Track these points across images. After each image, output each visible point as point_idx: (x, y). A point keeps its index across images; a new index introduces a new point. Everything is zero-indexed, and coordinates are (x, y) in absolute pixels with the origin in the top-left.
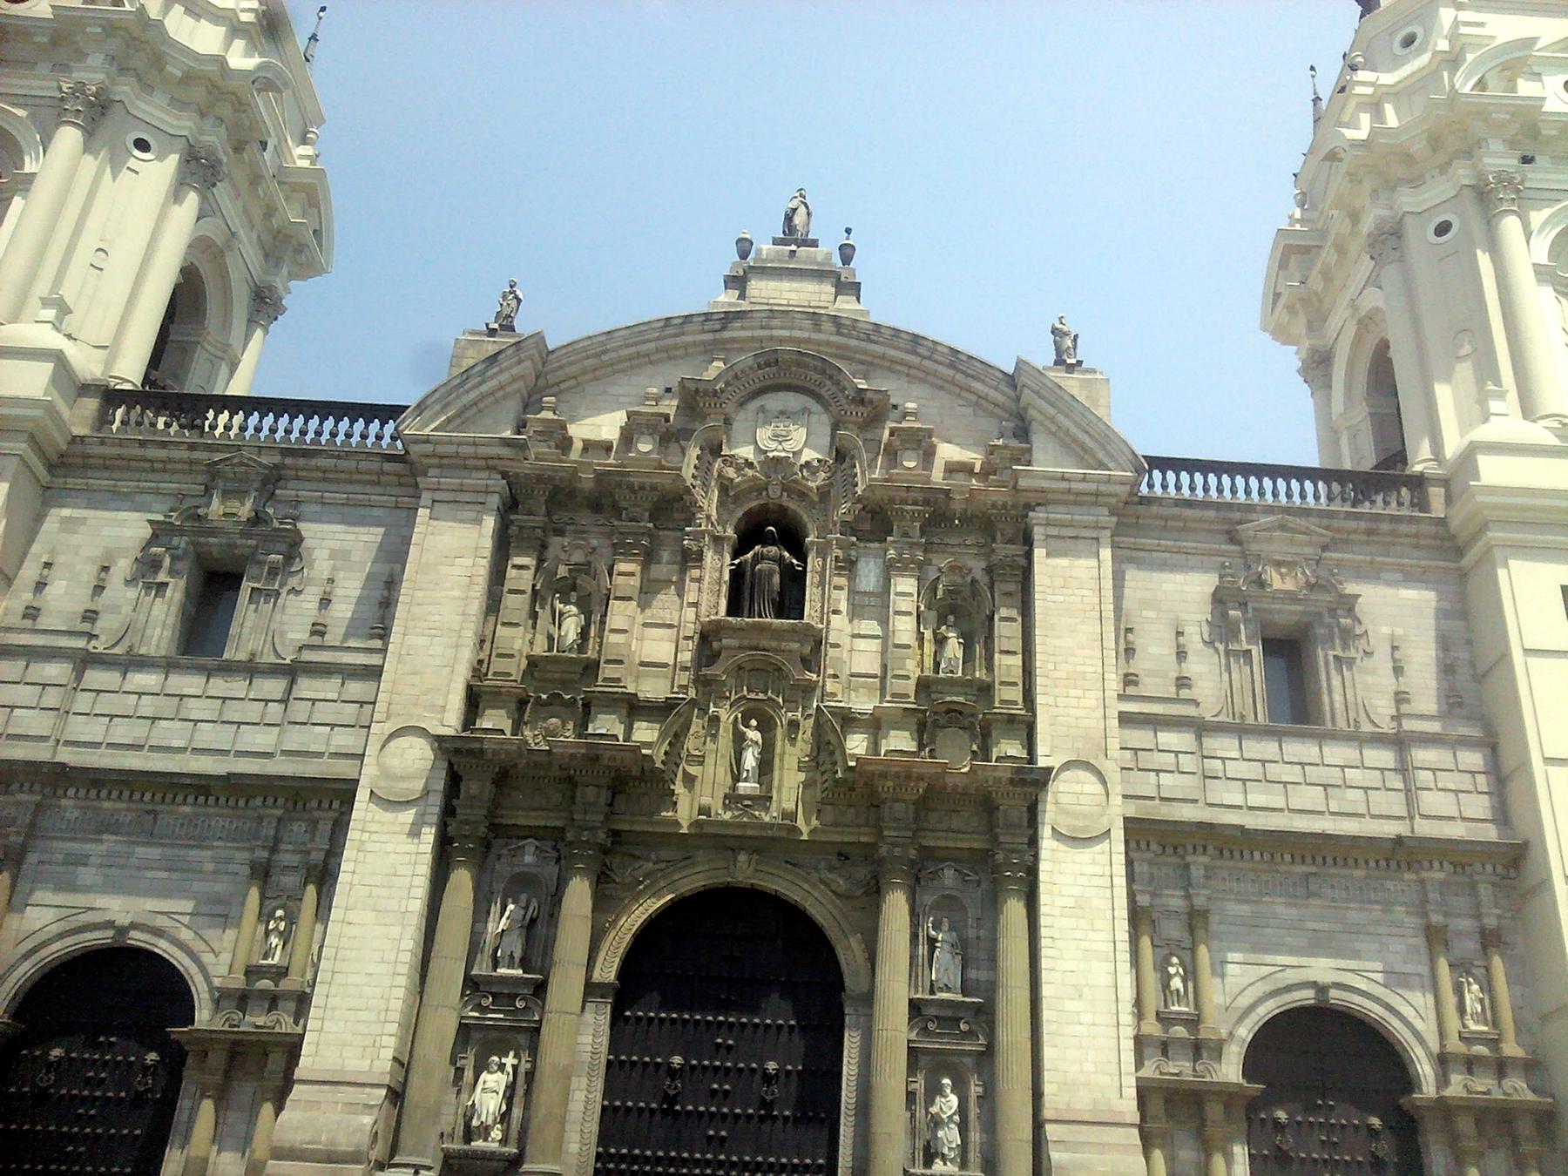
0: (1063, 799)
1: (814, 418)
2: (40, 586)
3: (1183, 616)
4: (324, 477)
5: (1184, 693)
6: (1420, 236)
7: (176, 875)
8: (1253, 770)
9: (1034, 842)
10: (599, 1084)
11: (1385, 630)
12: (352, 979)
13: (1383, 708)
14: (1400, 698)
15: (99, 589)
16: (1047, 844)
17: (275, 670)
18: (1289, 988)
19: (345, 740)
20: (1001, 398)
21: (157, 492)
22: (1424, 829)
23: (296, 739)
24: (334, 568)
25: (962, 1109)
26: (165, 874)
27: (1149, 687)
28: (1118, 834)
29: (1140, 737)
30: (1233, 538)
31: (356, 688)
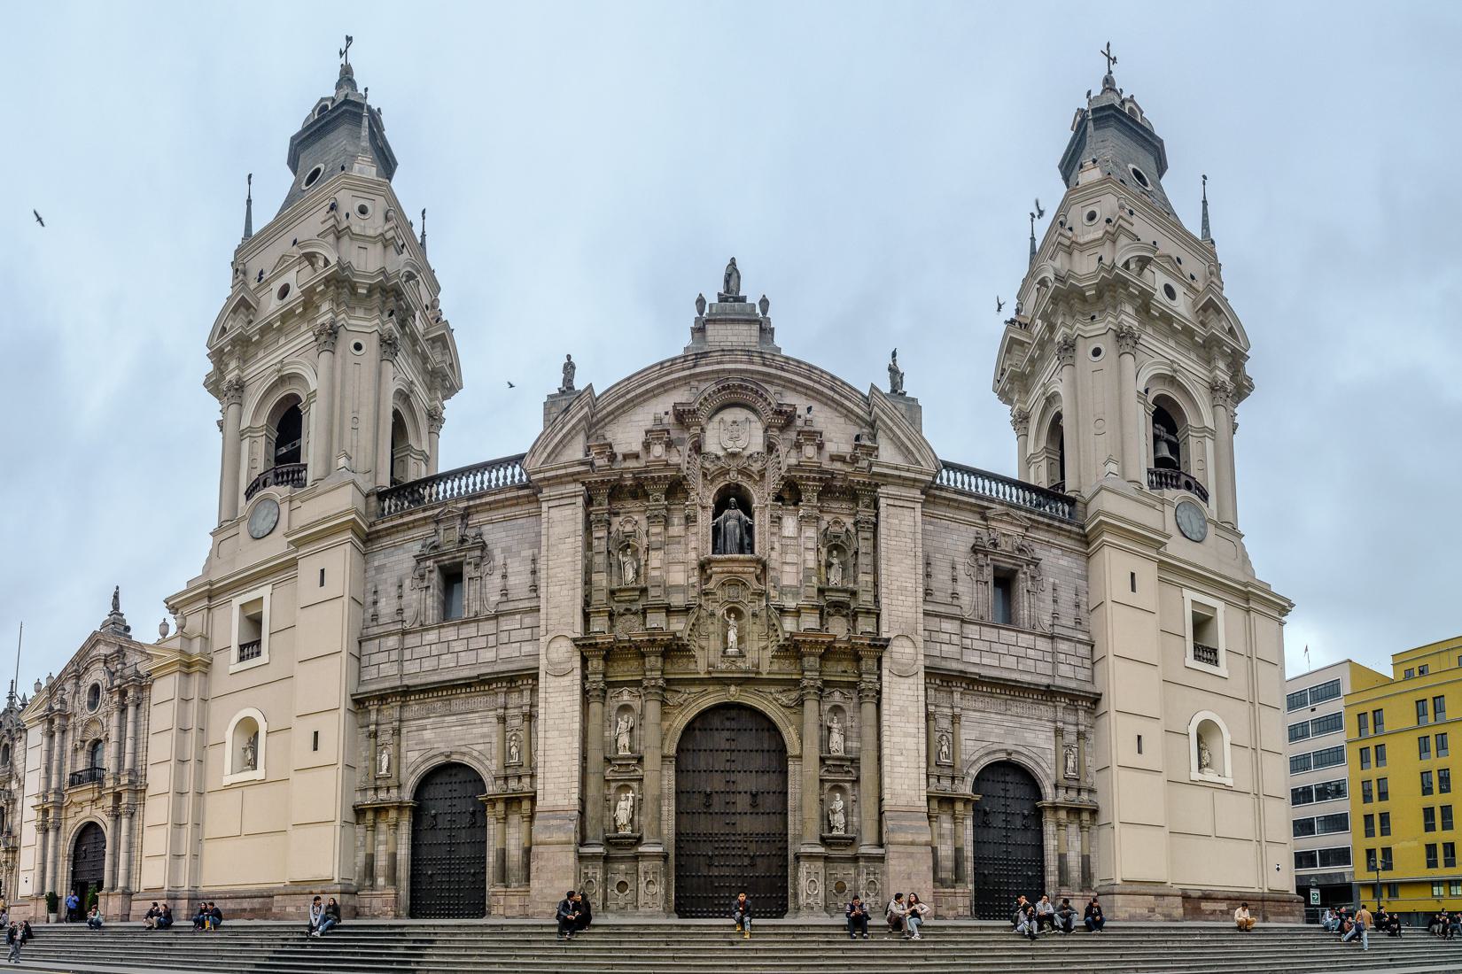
1: (753, 425)
3: (956, 559)
4: (491, 506)
5: (955, 602)
7: (465, 727)
8: (985, 646)
12: (553, 764)
17: (488, 619)
18: (995, 752)
24: (505, 558)
26: (460, 728)
27: (939, 596)
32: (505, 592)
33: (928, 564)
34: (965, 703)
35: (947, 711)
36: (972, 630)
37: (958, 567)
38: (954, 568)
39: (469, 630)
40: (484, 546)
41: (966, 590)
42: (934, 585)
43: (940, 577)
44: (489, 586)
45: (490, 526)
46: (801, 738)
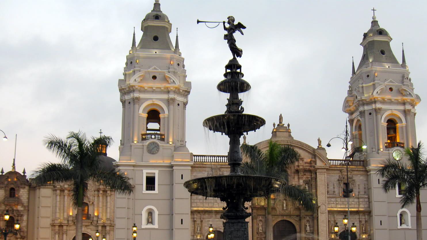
6: (367, 114)
8: (341, 203)
9: (318, 214)
11: (358, 183)
13: (357, 194)
14: (359, 192)
16: (319, 214)
21: (205, 171)
27: (330, 192)
28: (327, 213)
29: (330, 199)
30: (341, 172)
33: (328, 185)
34: (337, 217)
36: (338, 199)
37: (335, 185)
38: (334, 185)
41: (337, 190)
42: (329, 190)
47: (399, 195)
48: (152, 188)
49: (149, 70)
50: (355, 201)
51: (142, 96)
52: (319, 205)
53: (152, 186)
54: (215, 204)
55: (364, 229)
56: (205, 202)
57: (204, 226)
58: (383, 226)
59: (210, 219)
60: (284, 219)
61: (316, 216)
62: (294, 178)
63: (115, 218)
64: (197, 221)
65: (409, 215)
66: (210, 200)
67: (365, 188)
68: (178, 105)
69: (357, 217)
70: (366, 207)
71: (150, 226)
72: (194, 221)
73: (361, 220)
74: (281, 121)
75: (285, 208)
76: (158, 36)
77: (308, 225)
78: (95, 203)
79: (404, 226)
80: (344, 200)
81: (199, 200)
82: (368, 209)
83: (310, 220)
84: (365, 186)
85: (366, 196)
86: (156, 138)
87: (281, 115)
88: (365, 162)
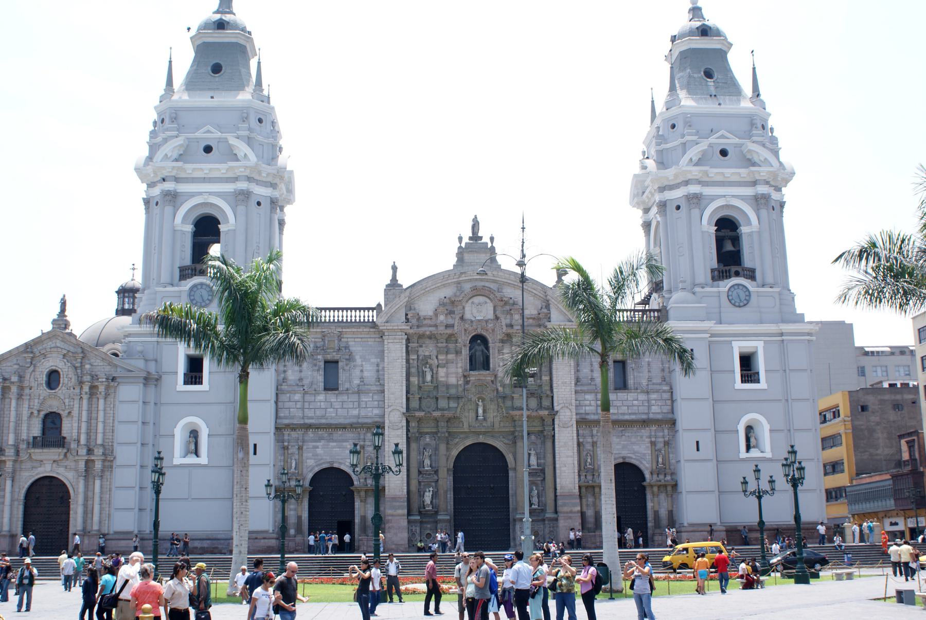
0: (561, 417)
2: (285, 372)
9: (554, 429)
10: (452, 493)
13: (644, 382)
15: (301, 371)
16: (556, 429)
19: (376, 411)
20: (542, 296)
22: (651, 416)
23: (363, 412)
24: (362, 361)
25: (538, 493)
27: (584, 381)
28: (575, 426)
31: (376, 397)
32: (362, 378)
35: (589, 440)
37: (594, 364)
39: (343, 397)
40: (351, 354)
42: (581, 375)
43: (584, 371)
44: (353, 375)
45: (353, 343)
46: (515, 459)
47: (742, 382)
48: (198, 380)
49: (196, 134)
50: (639, 399)
51: (183, 188)
52: (556, 408)
53: (198, 374)
54: (328, 410)
55: (660, 460)
56: (308, 407)
57: (304, 458)
58: (701, 455)
59: (318, 444)
60: (481, 441)
61: (549, 433)
62: (500, 351)
63: (115, 445)
64: (290, 447)
65: (766, 427)
66: (319, 404)
67: (663, 370)
68: (259, 204)
69: (645, 432)
70: (665, 411)
71: (192, 460)
72: (285, 448)
73: (653, 439)
74: (476, 230)
75: (481, 418)
76: (222, 63)
77: (533, 452)
78: (75, 413)
79: (754, 453)
80: (615, 396)
81: (294, 403)
82: (670, 416)
83: (539, 442)
84: (663, 364)
85: (666, 388)
86: (209, 275)
87: (476, 217)
88: (663, 312)
